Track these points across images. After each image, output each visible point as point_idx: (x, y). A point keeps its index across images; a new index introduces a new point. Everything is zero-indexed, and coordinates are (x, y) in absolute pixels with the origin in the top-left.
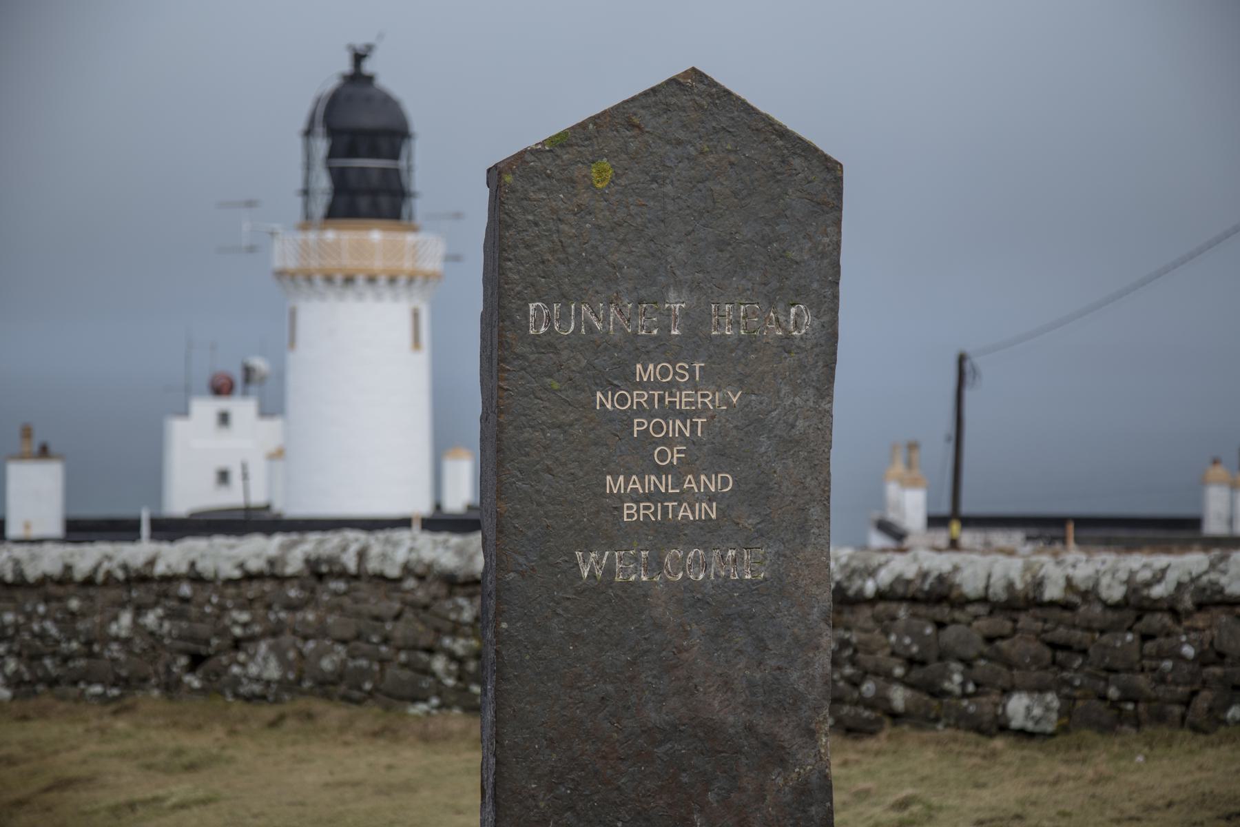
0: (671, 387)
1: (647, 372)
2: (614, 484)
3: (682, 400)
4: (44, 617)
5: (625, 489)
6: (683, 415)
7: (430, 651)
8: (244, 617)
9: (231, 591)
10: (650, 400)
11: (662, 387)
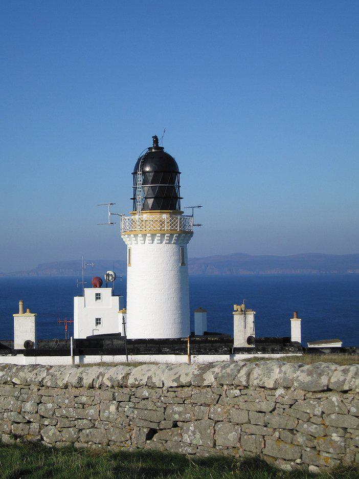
4: (67, 407)
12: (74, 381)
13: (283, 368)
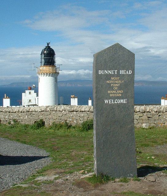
0: (116, 80)
1: (112, 78)
2: (109, 92)
3: (117, 82)
11: (114, 80)
12: (17, 111)
13: (64, 106)
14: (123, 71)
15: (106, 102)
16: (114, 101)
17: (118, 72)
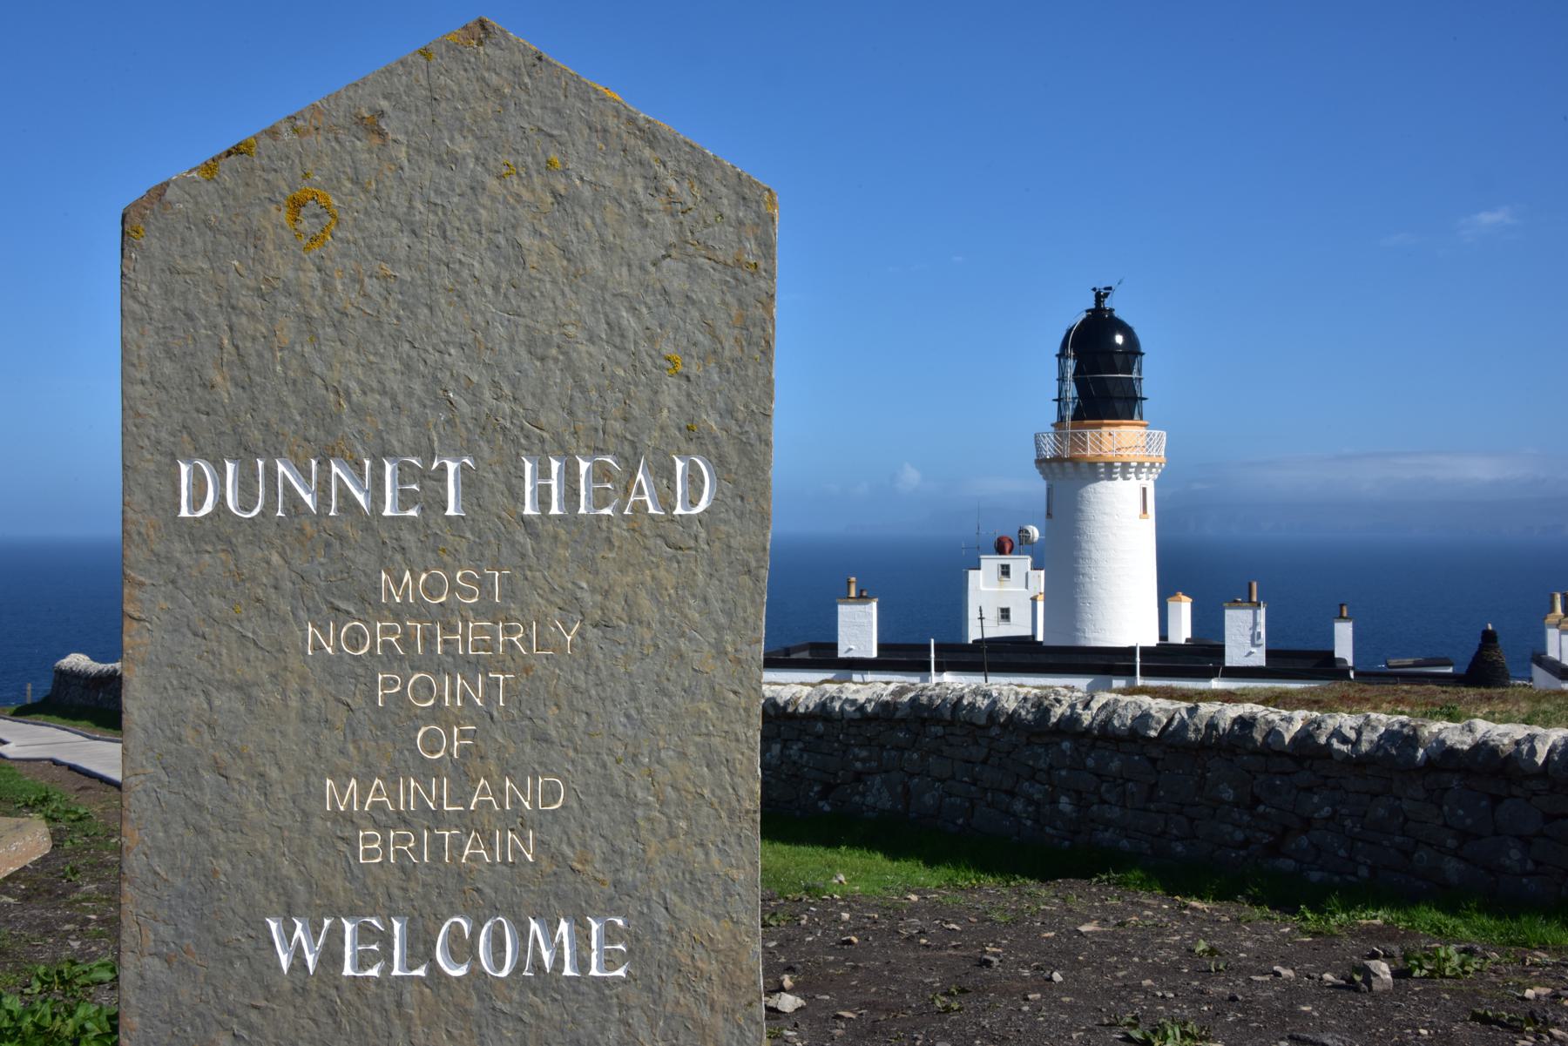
3: (467, 637)
5: (362, 803)
6: (472, 666)
7: (1012, 794)
8: (864, 754)
9: (853, 730)
10: (408, 640)
14: (570, 474)
15: (284, 961)
16: (420, 949)
17: (492, 489)
